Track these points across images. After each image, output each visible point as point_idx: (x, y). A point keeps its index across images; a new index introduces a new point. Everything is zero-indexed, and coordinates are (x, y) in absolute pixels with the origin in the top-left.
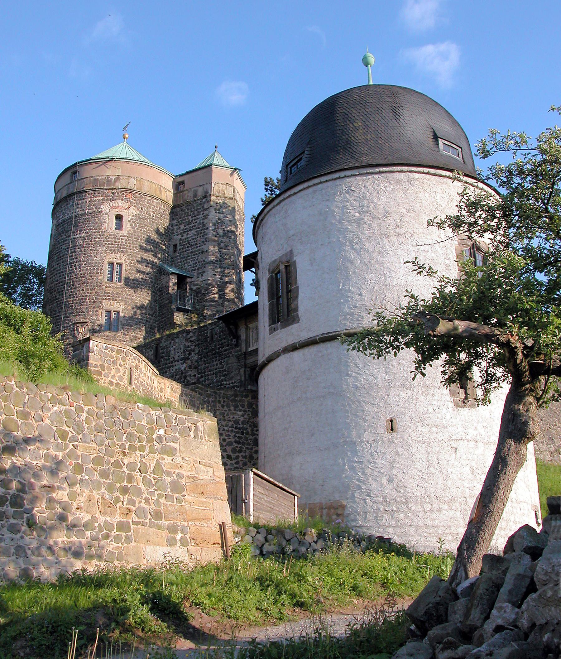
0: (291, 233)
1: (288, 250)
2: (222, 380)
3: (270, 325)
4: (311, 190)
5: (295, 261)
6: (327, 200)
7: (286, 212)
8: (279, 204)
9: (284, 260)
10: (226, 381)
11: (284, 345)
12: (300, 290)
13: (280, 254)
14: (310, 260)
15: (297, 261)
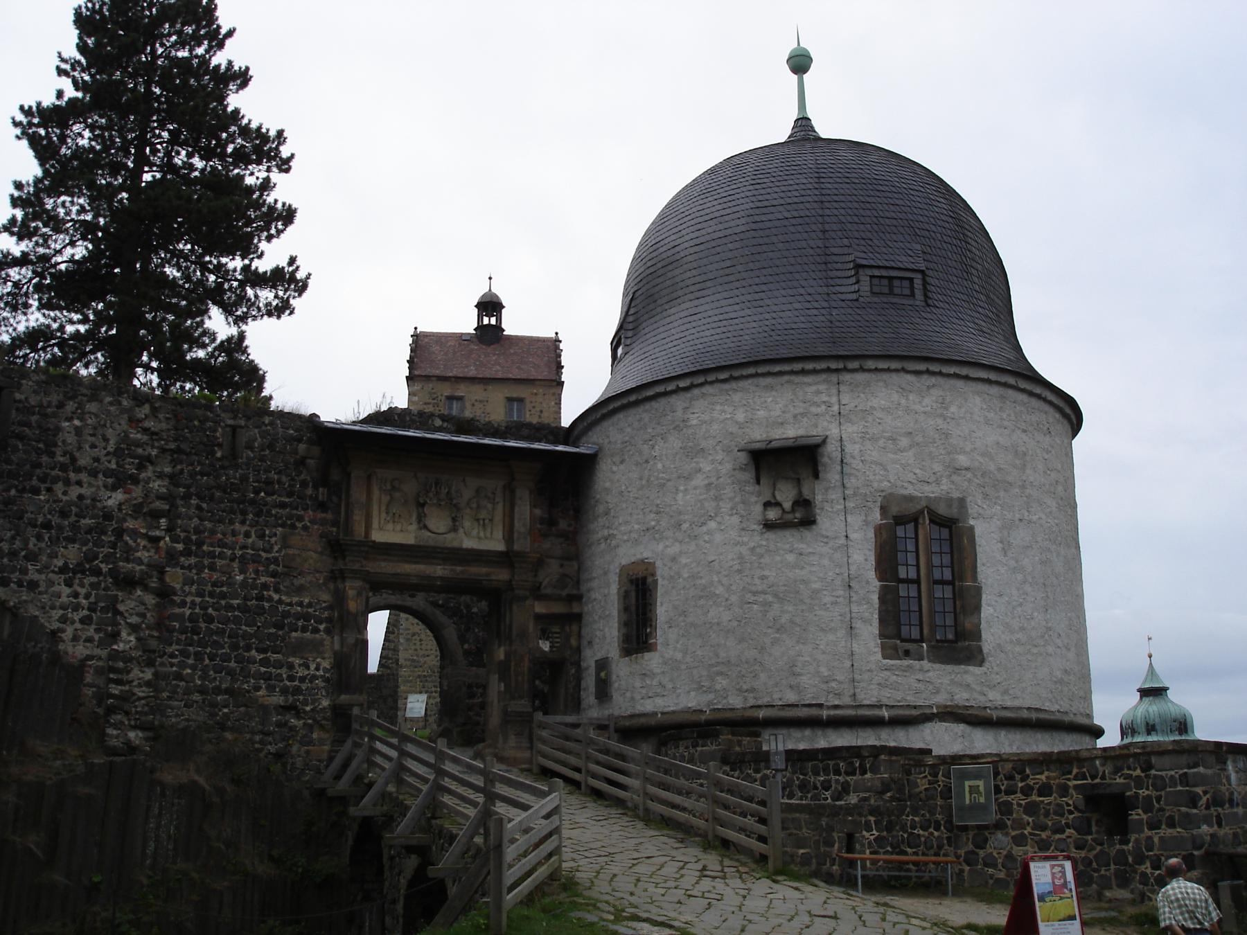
0: (963, 460)
1: (956, 495)
2: (265, 586)
3: (882, 635)
4: (995, 390)
5: (972, 528)
6: (1024, 431)
7: (944, 404)
8: (917, 373)
9: (942, 510)
10: (277, 591)
11: (941, 699)
12: (984, 597)
13: (931, 491)
14: (1001, 542)
15: (978, 532)
